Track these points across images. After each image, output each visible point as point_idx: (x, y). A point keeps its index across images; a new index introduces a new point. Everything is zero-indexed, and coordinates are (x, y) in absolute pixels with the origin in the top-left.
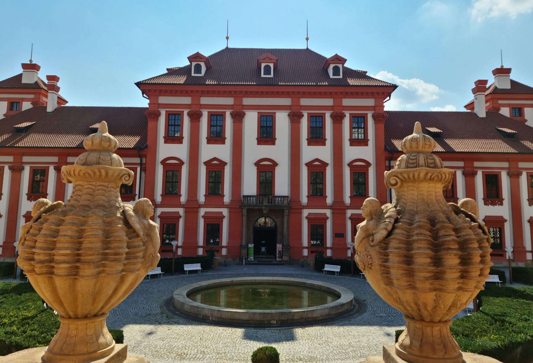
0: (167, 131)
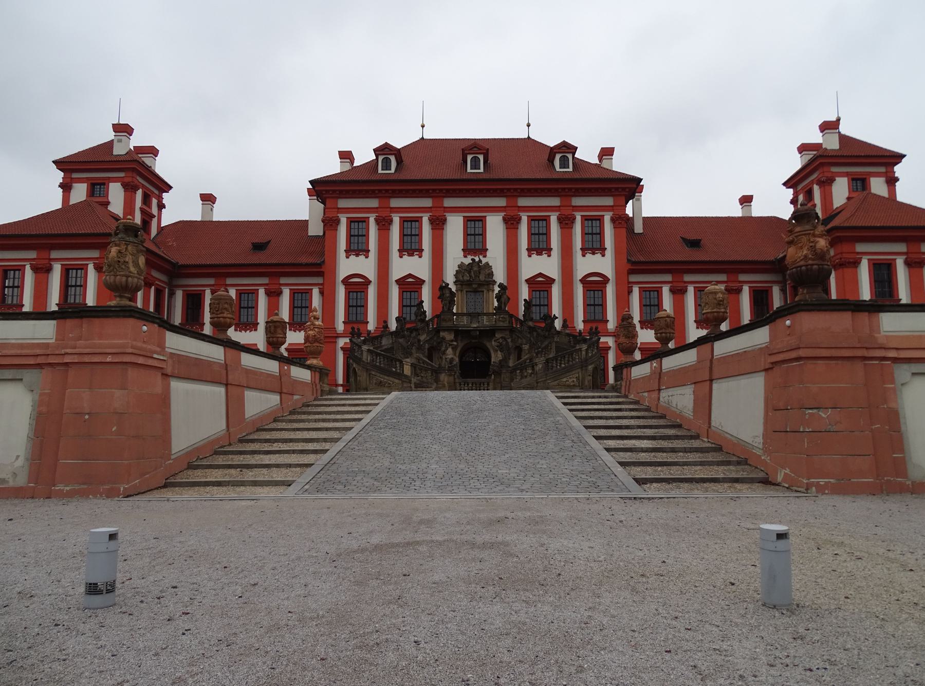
0: (349, 242)
